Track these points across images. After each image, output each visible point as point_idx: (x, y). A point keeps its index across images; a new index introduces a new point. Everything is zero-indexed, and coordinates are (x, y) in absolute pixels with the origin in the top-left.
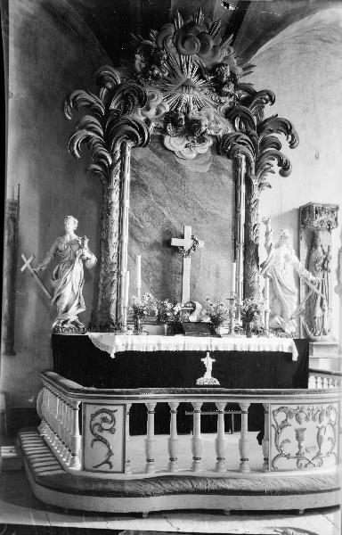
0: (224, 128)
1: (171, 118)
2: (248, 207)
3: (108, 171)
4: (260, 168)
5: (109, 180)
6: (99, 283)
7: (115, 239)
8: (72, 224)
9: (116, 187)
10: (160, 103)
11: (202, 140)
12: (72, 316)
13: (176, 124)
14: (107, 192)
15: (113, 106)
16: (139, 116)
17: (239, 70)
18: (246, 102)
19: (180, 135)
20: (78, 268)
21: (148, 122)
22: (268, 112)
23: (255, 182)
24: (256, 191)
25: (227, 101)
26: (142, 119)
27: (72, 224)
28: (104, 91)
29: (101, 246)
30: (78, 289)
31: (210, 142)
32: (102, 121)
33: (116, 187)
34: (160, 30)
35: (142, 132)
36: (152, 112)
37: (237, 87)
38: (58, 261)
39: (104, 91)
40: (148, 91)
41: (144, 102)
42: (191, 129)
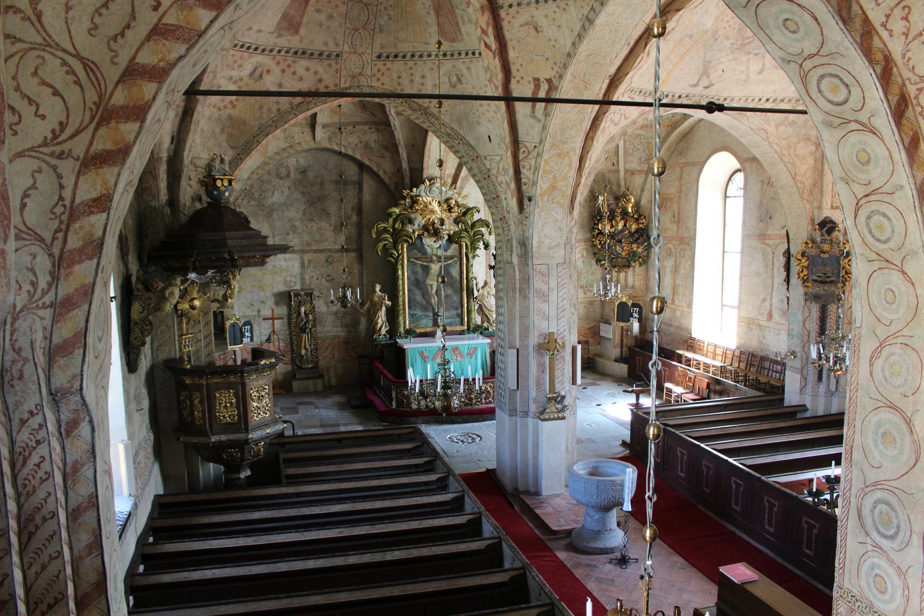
0: (454, 228)
1: (425, 228)
2: (467, 268)
3: (397, 259)
4: (474, 248)
5: (397, 263)
6: (392, 315)
7: (401, 293)
8: (378, 288)
9: (400, 267)
10: (420, 221)
11: (441, 238)
12: (383, 331)
13: (428, 231)
14: (396, 270)
15: (396, 226)
16: (410, 229)
17: (460, 200)
18: (465, 214)
19: (432, 236)
20: (384, 309)
21: (414, 232)
22: (476, 217)
23: (470, 256)
24: (471, 259)
25: (454, 215)
26: (411, 231)
27: (378, 288)
28: (391, 220)
29: (394, 297)
30: (384, 318)
31: (446, 237)
32: (392, 236)
33: (400, 267)
34: (417, 188)
35: (411, 238)
36: (416, 227)
37: (459, 206)
38: (374, 309)
39: (391, 220)
40: (413, 216)
41: (411, 222)
42: (436, 234)
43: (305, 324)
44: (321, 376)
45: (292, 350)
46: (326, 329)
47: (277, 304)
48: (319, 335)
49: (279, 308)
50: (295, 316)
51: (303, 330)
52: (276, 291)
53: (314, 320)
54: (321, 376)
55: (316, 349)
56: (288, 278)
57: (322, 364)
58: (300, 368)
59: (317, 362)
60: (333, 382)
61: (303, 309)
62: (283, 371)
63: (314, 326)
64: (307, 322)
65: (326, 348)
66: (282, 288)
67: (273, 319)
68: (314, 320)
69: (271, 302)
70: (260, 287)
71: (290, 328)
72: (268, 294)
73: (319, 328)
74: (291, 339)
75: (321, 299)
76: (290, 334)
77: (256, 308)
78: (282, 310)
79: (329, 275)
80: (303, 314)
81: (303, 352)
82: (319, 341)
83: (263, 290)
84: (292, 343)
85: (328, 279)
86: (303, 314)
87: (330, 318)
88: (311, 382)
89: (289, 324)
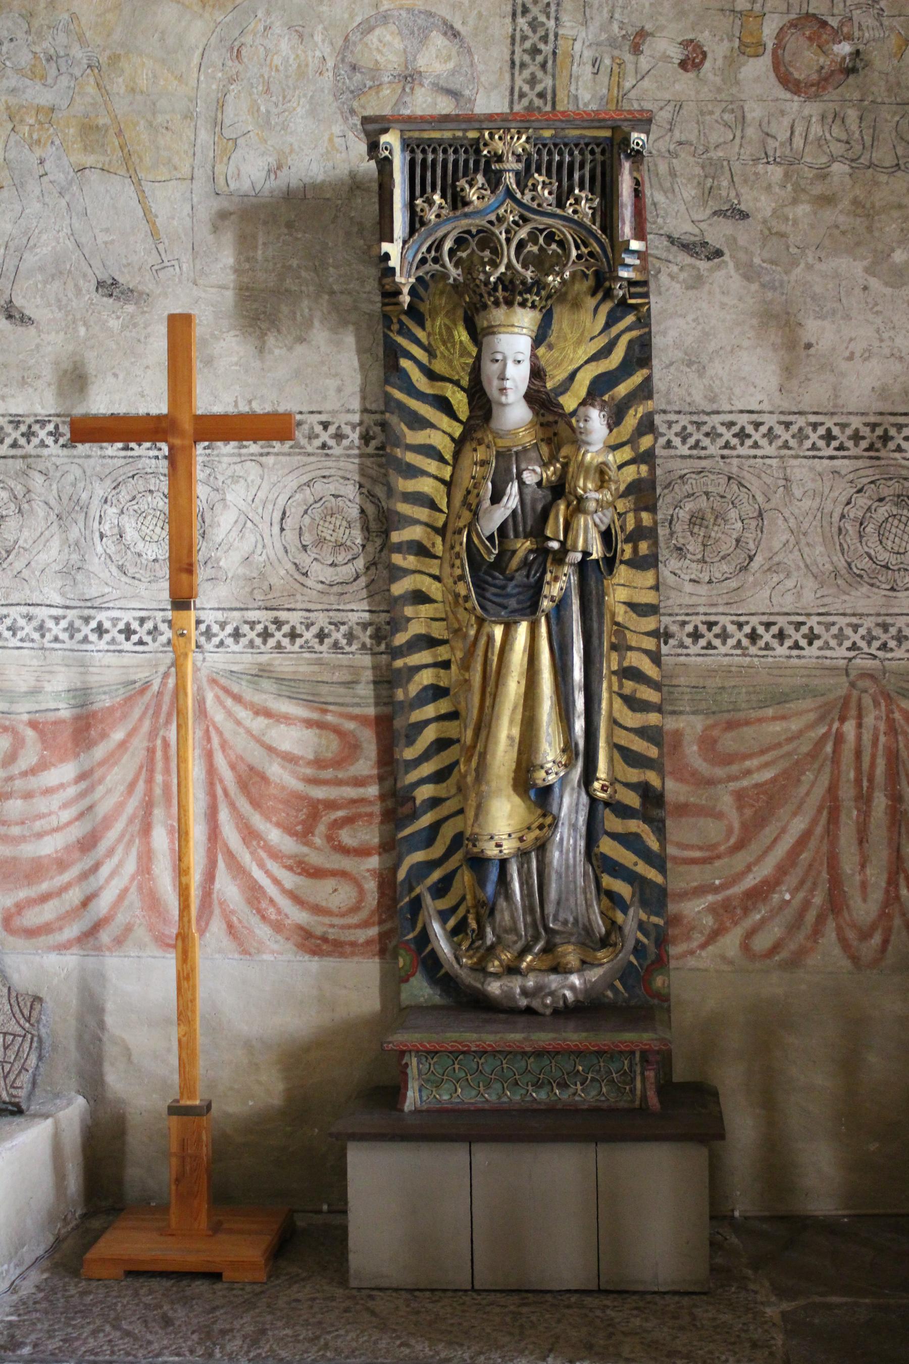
43: (534, 521)
44: (684, 1110)
45: (397, 806)
46: (762, 598)
47: (261, 310)
48: (688, 659)
49: (285, 358)
50: (442, 433)
51: (503, 579)
52: (251, 171)
53: (643, 494)
54: (684, 1110)
55: (652, 798)
56: (386, 48)
57: (706, 971)
58: (470, 1003)
59: (654, 954)
60: (822, 1177)
61: (514, 342)
62: (295, 1022)
63: (635, 545)
64: (558, 489)
65: (761, 808)
66: (325, 151)
67: (176, 432)
68: (643, 494)
69: (206, 284)
70: (90, 131)
71: (380, 571)
72: (179, 205)
73: (686, 585)
74: (387, 681)
75: (725, 277)
76: (383, 631)
77: (49, 344)
78: (321, 374)
79: (813, 26)
80: (515, 413)
81: (503, 821)
82: (689, 725)
83: (129, 165)
84: (389, 730)
85: (807, 61)
86: (515, 413)
87: (814, 487)
88: (559, 1172)
89: (379, 523)
